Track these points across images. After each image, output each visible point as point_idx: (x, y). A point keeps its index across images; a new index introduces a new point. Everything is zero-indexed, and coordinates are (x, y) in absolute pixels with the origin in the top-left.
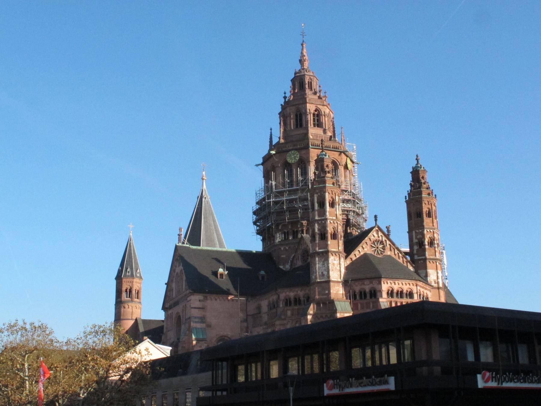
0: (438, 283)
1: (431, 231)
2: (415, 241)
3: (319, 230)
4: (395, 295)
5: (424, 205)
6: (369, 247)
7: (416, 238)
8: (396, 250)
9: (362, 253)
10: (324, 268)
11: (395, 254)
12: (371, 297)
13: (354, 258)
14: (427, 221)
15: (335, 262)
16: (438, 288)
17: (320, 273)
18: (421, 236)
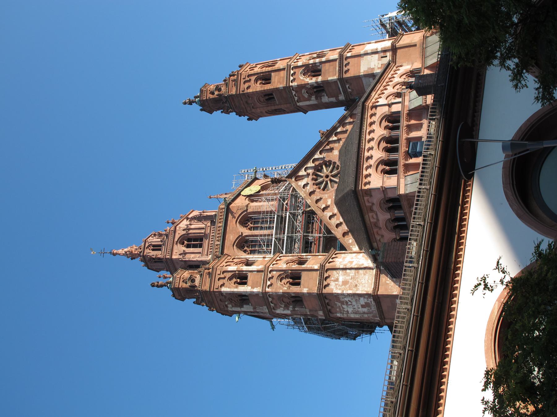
0: (385, 51)
1: (292, 72)
2: (313, 101)
3: (286, 307)
4: (393, 156)
5: (250, 90)
6: (325, 195)
7: (309, 99)
8: (331, 139)
9: (336, 211)
10: (354, 303)
11: (339, 140)
12: (400, 207)
13: (344, 228)
14: (278, 82)
15: (341, 279)
16: (394, 49)
17: (365, 310)
18: (303, 91)
